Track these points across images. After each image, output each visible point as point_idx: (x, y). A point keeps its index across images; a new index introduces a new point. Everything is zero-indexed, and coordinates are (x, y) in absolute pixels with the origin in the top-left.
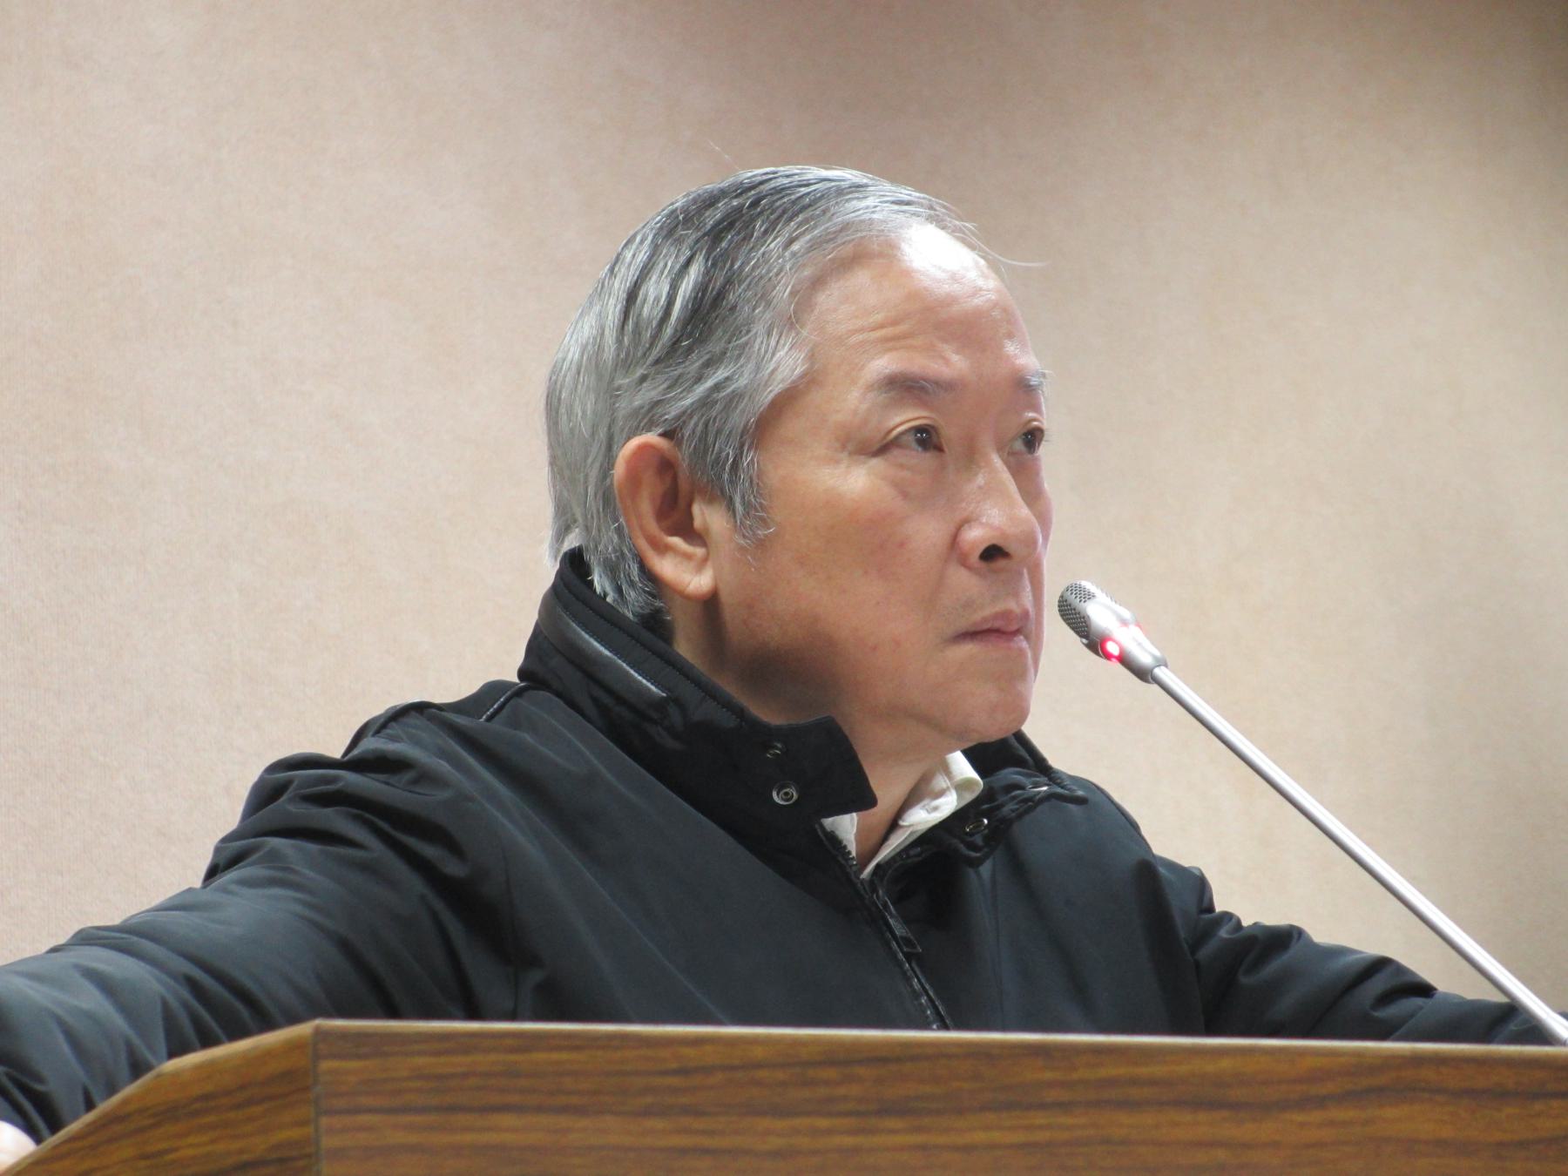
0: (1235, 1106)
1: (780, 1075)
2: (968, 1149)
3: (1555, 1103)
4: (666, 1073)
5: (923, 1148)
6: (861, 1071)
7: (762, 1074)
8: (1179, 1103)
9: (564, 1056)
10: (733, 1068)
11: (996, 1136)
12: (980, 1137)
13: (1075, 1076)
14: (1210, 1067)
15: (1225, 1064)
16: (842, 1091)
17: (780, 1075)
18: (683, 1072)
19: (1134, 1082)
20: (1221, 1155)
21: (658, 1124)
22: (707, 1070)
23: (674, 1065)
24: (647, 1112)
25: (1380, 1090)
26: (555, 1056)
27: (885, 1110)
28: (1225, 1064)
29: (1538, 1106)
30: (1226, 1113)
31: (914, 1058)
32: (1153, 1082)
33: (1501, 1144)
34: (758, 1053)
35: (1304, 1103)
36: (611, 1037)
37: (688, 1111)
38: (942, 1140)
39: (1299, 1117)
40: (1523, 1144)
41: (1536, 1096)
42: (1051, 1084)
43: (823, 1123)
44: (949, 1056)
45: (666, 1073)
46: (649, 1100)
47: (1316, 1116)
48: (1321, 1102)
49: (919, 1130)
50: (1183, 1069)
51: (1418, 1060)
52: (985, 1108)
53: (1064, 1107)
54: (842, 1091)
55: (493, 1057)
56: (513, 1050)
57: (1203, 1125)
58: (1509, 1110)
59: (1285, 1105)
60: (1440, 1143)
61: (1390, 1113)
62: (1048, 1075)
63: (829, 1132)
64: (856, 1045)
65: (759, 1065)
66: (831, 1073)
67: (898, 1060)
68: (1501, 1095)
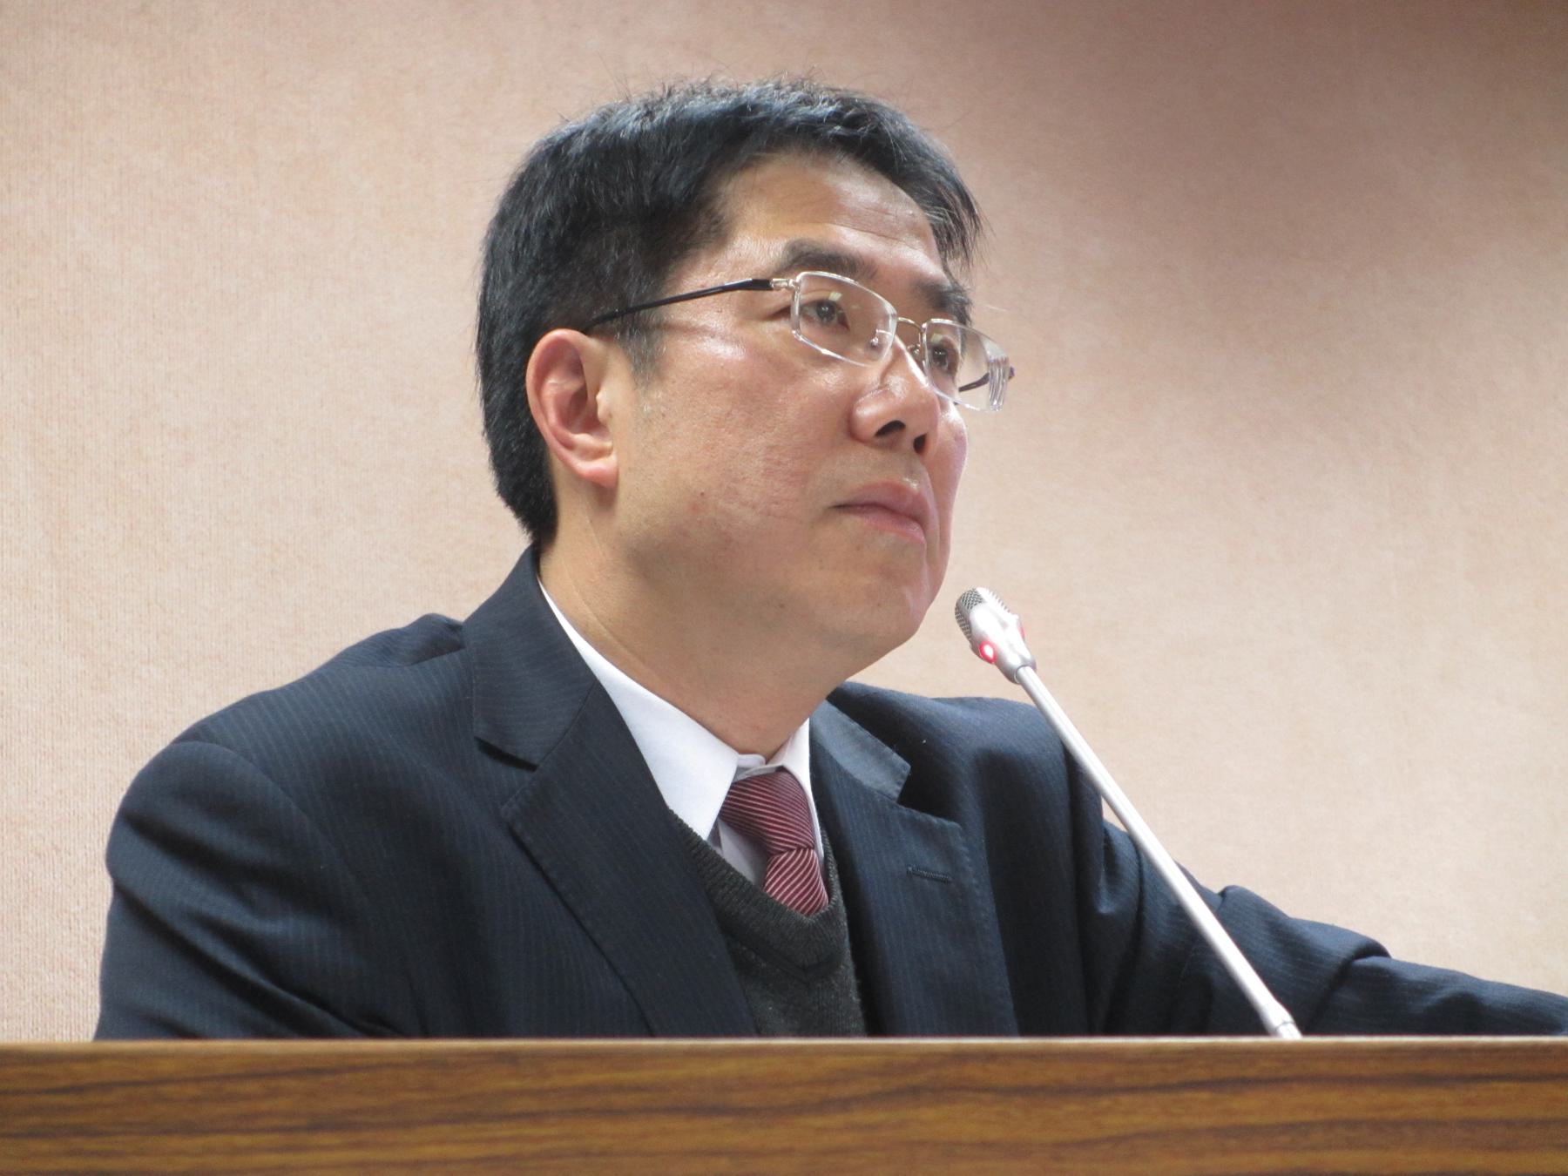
0: (741, 1112)
1: (191, 1090)
2: (417, 1164)
3: (1126, 1100)
4: (49, 1091)
5: (362, 1165)
6: (290, 1084)
7: (167, 1090)
8: (673, 1110)
10: (137, 1084)
11: (452, 1151)
12: (432, 1151)
13: (547, 1084)
14: (710, 1070)
16: (264, 1106)
17: (191, 1090)
18: (78, 1089)
19: (620, 1088)
20: (723, 1164)
21: (45, 1146)
22: (106, 1087)
23: (62, 1083)
24: (33, 1134)
27: (317, 1126)
28: (730, 1067)
29: (1105, 1102)
30: (729, 1120)
31: (354, 1069)
32: (638, 1088)
33: (1058, 1145)
34: (167, 1067)
35: (823, 1106)
37: (80, 1131)
38: (382, 1155)
39: (819, 1122)
40: (1086, 1144)
41: (1097, 1091)
42: (522, 1093)
43: (242, 1140)
44: (397, 1066)
45: (49, 1091)
46: (35, 1120)
47: (838, 1120)
48: (845, 1104)
49: (359, 1145)
50: (679, 1073)
51: (961, 1056)
52: (436, 1121)
53: (535, 1117)
54: (264, 1106)
57: (701, 1133)
58: (1072, 1108)
59: (799, 1109)
60: (985, 1145)
61: (928, 1114)
62: (514, 1084)
63: (250, 1150)
64: (284, 1058)
66: (252, 1087)
67: (334, 1071)
68: (1063, 1091)
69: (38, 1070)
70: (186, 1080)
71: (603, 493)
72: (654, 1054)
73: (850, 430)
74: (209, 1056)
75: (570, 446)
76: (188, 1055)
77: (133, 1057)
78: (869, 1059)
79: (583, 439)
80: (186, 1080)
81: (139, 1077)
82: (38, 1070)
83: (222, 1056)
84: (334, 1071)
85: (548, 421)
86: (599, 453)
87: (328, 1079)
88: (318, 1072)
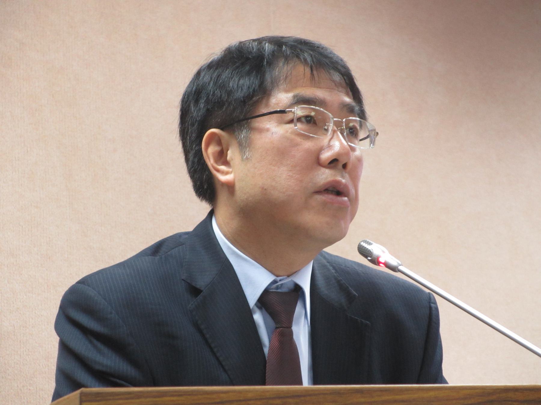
9: (175, 398)
10: (240, 401)
13: (373, 400)
14: (426, 395)
15: (432, 394)
19: (395, 401)
23: (218, 400)
25: (492, 401)
26: (172, 398)
28: (432, 394)
31: (310, 395)
34: (250, 395)
36: (193, 391)
50: (416, 396)
55: (148, 400)
56: (155, 397)
64: (288, 391)
65: (250, 400)
67: (304, 396)
69: (208, 396)
70: (256, 399)
71: (230, 187)
72: (407, 389)
73: (318, 163)
74: (264, 391)
75: (218, 171)
76: (257, 391)
77: (240, 392)
78: (477, 391)
79: (223, 168)
80: (256, 399)
81: (241, 399)
82: (208, 396)
83: (268, 391)
84: (304, 396)
85: (210, 162)
86: (227, 173)
87: (303, 398)
88: (299, 396)
